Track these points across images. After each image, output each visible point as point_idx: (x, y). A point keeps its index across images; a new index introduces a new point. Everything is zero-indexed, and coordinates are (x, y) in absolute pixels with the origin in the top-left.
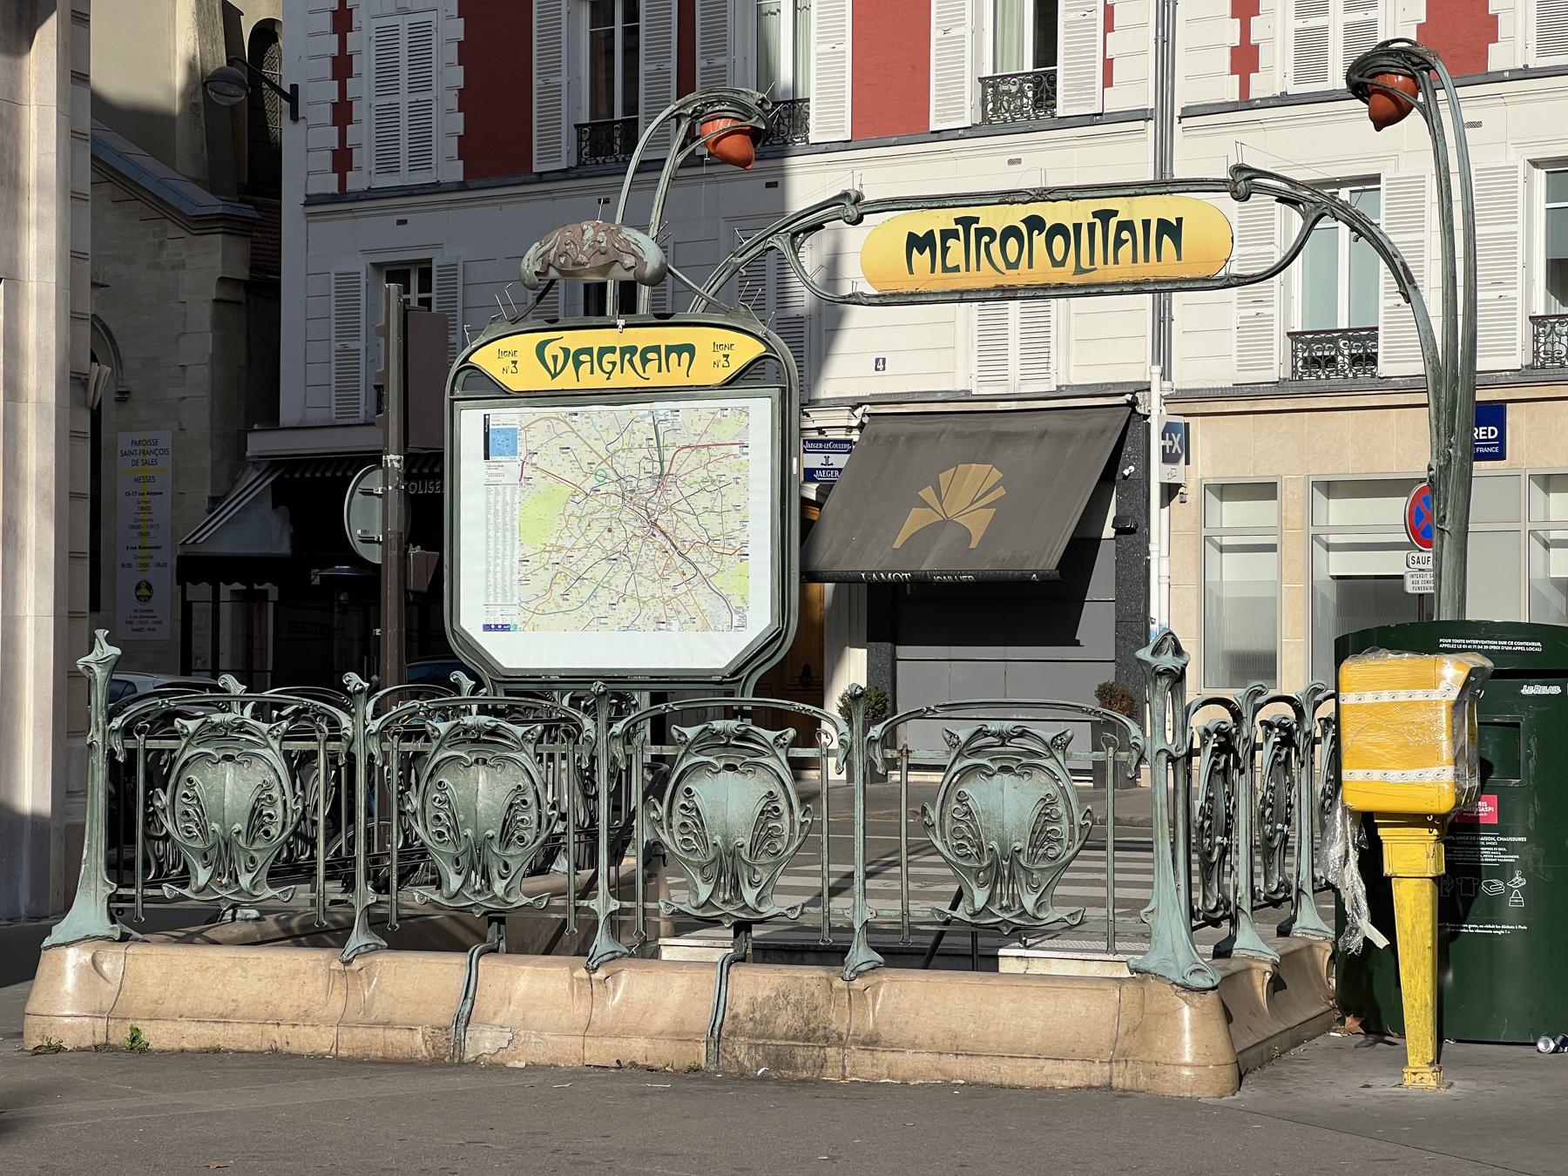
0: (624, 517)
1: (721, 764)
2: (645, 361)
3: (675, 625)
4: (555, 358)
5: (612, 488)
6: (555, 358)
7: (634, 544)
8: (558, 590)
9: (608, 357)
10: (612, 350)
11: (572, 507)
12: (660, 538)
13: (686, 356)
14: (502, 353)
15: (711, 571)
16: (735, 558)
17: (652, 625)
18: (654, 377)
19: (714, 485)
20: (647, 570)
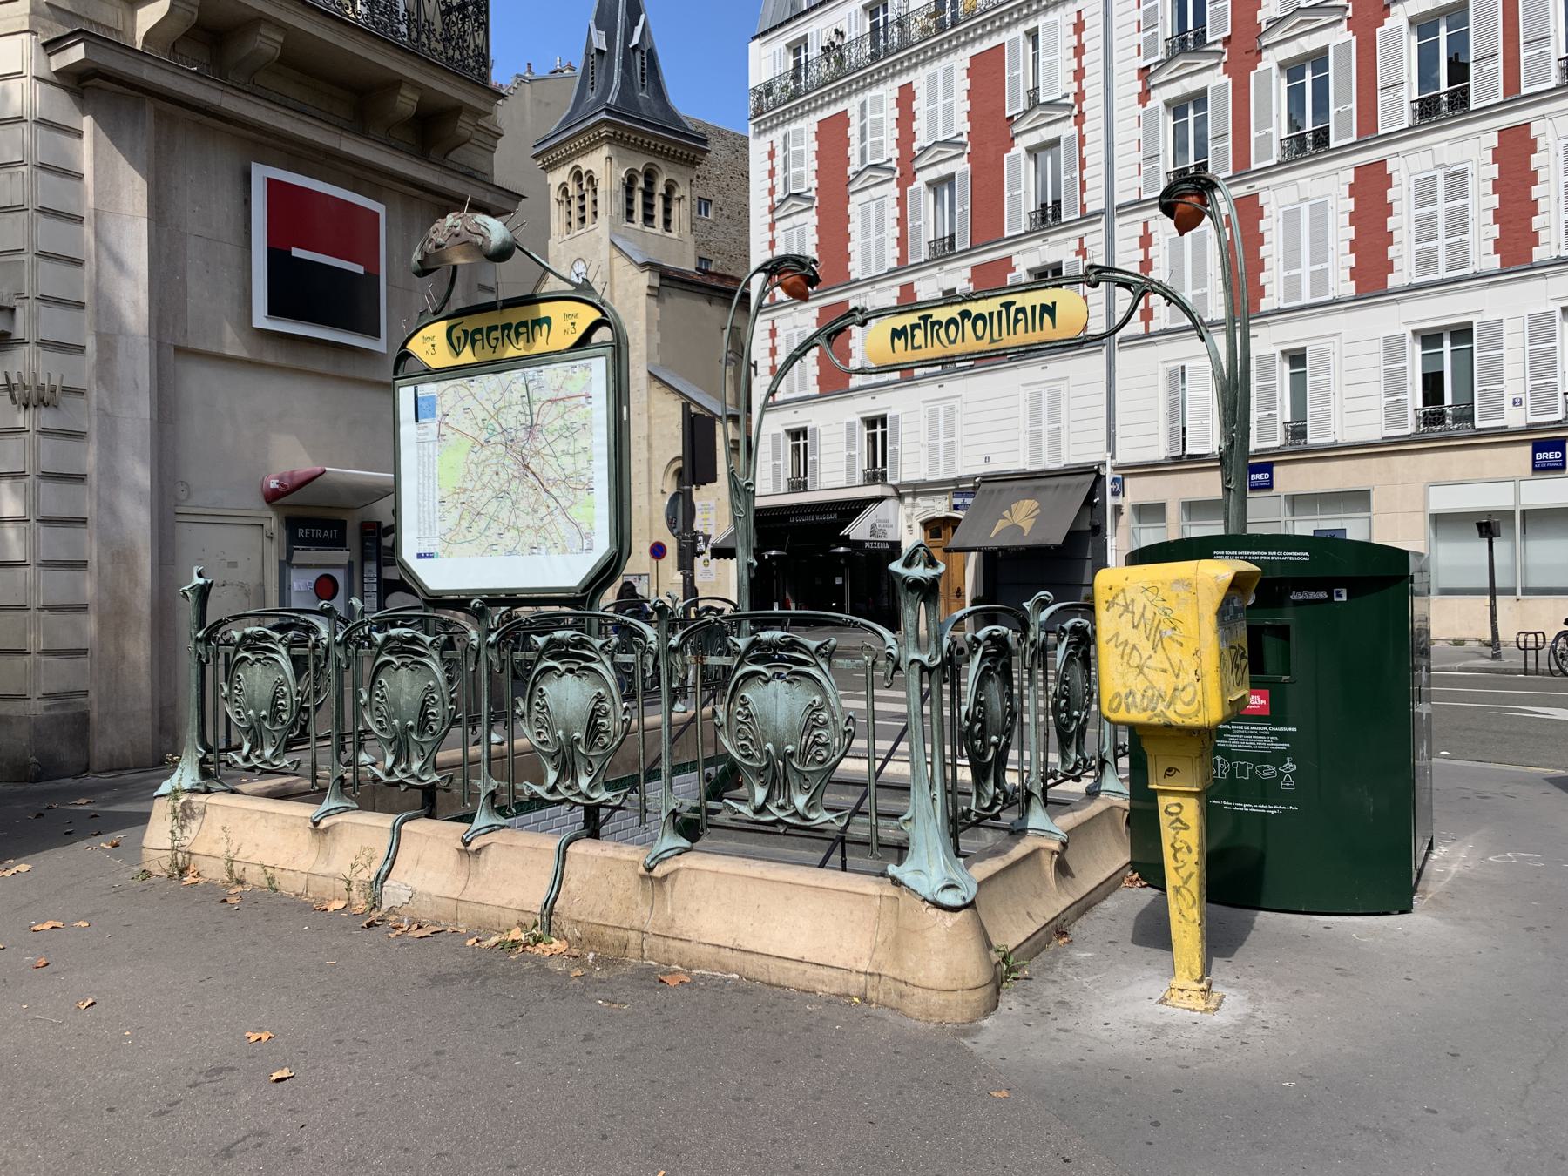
0: (507, 462)
1: (563, 668)
2: (518, 334)
3: (543, 550)
5: (498, 438)
7: (514, 484)
8: (465, 524)
9: (494, 334)
10: (495, 328)
11: (472, 456)
12: (531, 478)
15: (567, 504)
16: (584, 492)
17: (527, 549)
19: (569, 432)
20: (523, 505)
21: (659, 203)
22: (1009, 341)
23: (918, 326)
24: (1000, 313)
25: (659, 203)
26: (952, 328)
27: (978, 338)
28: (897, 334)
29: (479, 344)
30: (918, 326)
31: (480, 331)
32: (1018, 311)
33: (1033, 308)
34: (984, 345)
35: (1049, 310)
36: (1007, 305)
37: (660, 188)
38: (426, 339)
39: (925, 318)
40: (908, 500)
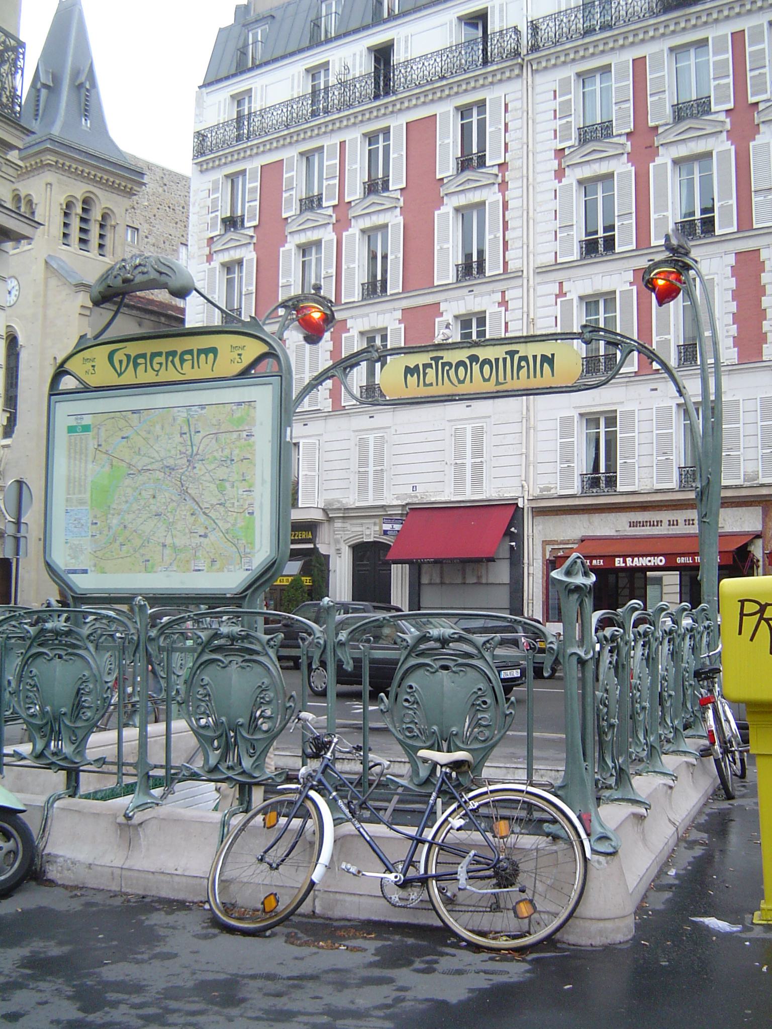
2: (182, 361)
4: (121, 362)
6: (121, 362)
9: (157, 359)
10: (159, 354)
13: (211, 356)
14: (86, 360)
18: (189, 372)
21: (95, 230)
22: (512, 384)
23: (430, 366)
24: (505, 360)
25: (95, 230)
26: (461, 369)
27: (485, 380)
28: (409, 371)
29: (141, 368)
30: (430, 366)
31: (143, 356)
32: (521, 359)
33: (535, 357)
34: (491, 387)
35: (549, 360)
36: (512, 353)
37: (96, 215)
38: (86, 360)
39: (436, 359)
40: (338, 524)
